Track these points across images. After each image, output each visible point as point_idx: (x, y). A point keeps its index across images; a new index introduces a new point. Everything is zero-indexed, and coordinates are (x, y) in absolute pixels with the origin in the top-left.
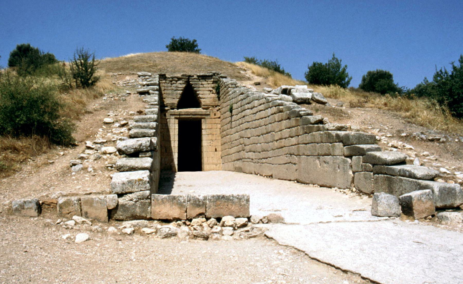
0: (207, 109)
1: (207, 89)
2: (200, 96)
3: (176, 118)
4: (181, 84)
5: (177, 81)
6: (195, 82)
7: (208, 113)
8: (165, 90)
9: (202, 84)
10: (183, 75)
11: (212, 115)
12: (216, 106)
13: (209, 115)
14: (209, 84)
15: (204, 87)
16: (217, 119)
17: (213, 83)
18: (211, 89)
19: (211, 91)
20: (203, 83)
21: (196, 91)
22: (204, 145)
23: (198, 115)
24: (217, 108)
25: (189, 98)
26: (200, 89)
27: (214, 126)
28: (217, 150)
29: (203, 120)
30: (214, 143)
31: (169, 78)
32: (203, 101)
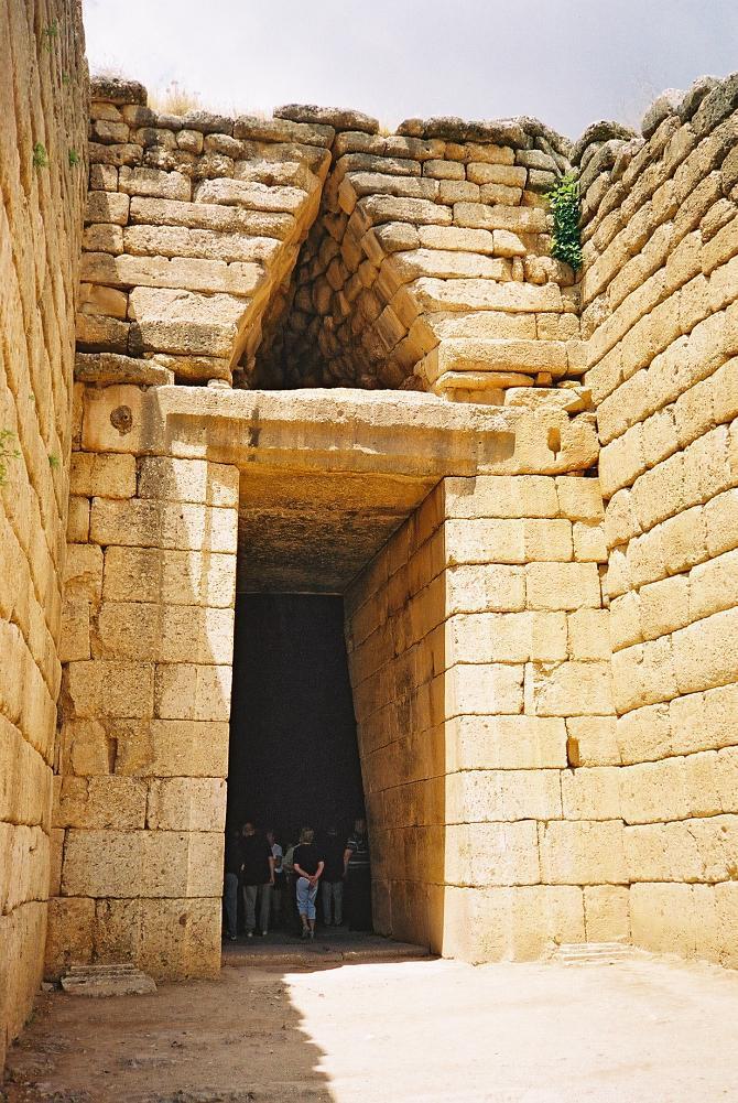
2: (430, 287)
3: (220, 455)
4: (269, 181)
5: (238, 157)
6: (396, 182)
8: (131, 221)
9: (438, 201)
10: (290, 114)
12: (557, 381)
13: (501, 443)
16: (572, 480)
17: (522, 202)
19: (510, 259)
20: (451, 191)
21: (392, 249)
24: (569, 394)
25: (326, 318)
27: (556, 538)
28: (585, 751)
30: (559, 692)
31: (176, 129)
32: (452, 339)
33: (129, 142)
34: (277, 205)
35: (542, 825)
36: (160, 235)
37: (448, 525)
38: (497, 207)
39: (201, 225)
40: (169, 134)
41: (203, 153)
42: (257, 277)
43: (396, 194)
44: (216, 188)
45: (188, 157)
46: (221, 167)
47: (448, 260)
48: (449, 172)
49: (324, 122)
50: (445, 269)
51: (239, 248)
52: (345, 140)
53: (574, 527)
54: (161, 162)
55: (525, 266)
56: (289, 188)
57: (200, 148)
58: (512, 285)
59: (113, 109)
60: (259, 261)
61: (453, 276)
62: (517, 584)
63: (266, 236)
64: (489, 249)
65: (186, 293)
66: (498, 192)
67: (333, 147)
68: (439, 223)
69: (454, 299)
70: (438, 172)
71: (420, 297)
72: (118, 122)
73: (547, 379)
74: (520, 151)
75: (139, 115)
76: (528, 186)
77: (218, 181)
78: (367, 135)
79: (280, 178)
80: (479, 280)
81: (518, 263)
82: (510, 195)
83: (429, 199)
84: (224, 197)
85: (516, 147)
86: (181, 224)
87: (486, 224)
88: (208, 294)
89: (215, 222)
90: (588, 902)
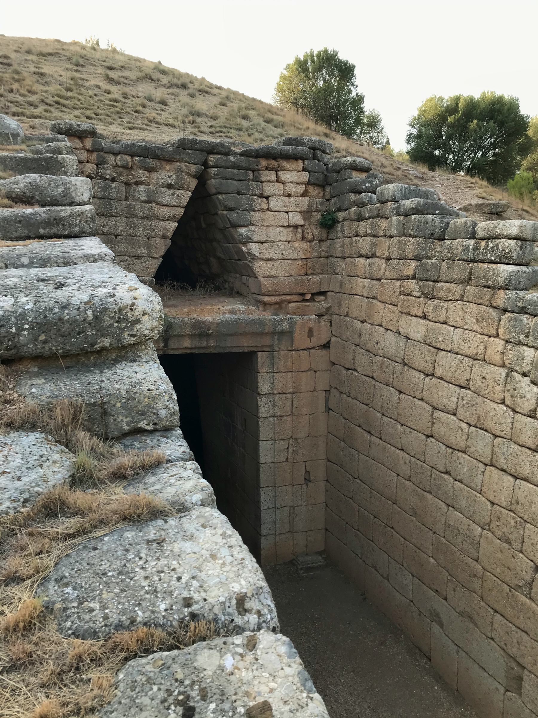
0: (279, 306)
1: (283, 219)
2: (255, 248)
4: (169, 186)
7: (286, 326)
9: (261, 196)
10: (183, 145)
11: (301, 339)
14: (289, 195)
15: (268, 209)
17: (305, 194)
18: (297, 219)
19: (296, 227)
20: (268, 189)
22: (262, 460)
23: (245, 334)
26: (255, 216)
29: (261, 357)
33: (88, 162)
34: (175, 204)
35: (292, 508)
36: (109, 223)
37: (259, 376)
38: (292, 199)
39: (133, 216)
40: (112, 157)
41: (132, 168)
42: (164, 248)
43: (239, 193)
44: (140, 193)
45: (125, 171)
46: (143, 179)
47: (264, 233)
48: (268, 178)
49: (201, 150)
50: (263, 238)
51: (154, 230)
52: (212, 159)
53: (317, 374)
54: (108, 177)
55: (303, 232)
56: (182, 192)
57: (130, 166)
58: (296, 244)
59: (77, 141)
60: (164, 237)
61: (267, 241)
62: (289, 404)
63: (168, 220)
64: (286, 224)
65: (126, 258)
66: (292, 188)
67: (205, 164)
68: (262, 210)
69: (267, 256)
70: (263, 179)
71: (249, 253)
72: (81, 149)
73: (308, 297)
74: (306, 162)
75: (93, 144)
76: (309, 183)
77: (142, 188)
78: (224, 158)
79: (176, 186)
80: (280, 244)
81: (300, 230)
82: (299, 191)
83: (256, 195)
84: (144, 198)
85: (303, 160)
86: (121, 216)
87: (285, 209)
88: (138, 257)
89: (140, 214)
90: (309, 538)
